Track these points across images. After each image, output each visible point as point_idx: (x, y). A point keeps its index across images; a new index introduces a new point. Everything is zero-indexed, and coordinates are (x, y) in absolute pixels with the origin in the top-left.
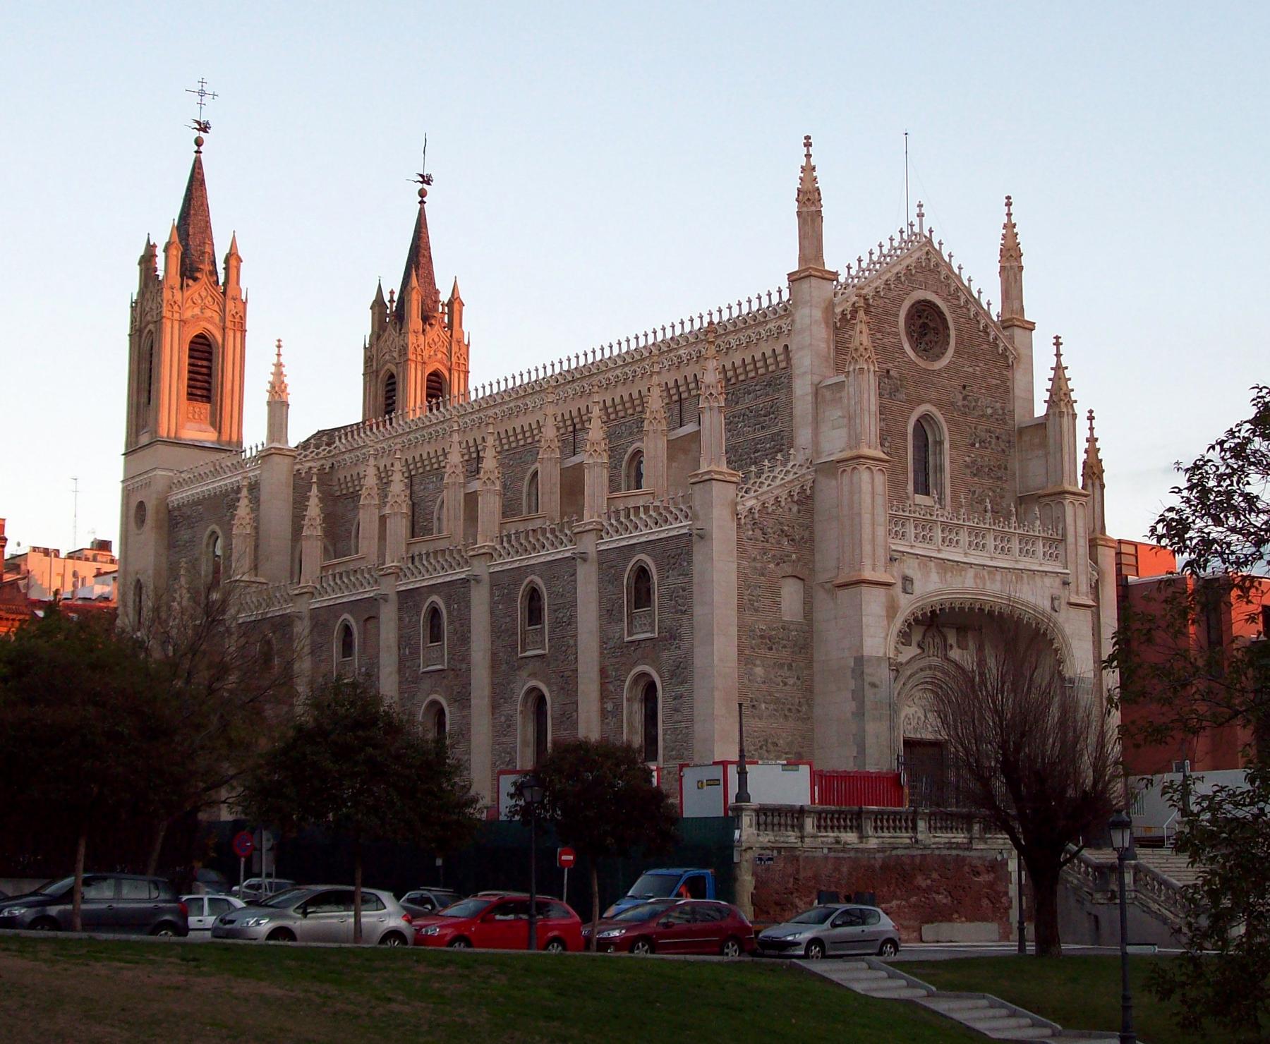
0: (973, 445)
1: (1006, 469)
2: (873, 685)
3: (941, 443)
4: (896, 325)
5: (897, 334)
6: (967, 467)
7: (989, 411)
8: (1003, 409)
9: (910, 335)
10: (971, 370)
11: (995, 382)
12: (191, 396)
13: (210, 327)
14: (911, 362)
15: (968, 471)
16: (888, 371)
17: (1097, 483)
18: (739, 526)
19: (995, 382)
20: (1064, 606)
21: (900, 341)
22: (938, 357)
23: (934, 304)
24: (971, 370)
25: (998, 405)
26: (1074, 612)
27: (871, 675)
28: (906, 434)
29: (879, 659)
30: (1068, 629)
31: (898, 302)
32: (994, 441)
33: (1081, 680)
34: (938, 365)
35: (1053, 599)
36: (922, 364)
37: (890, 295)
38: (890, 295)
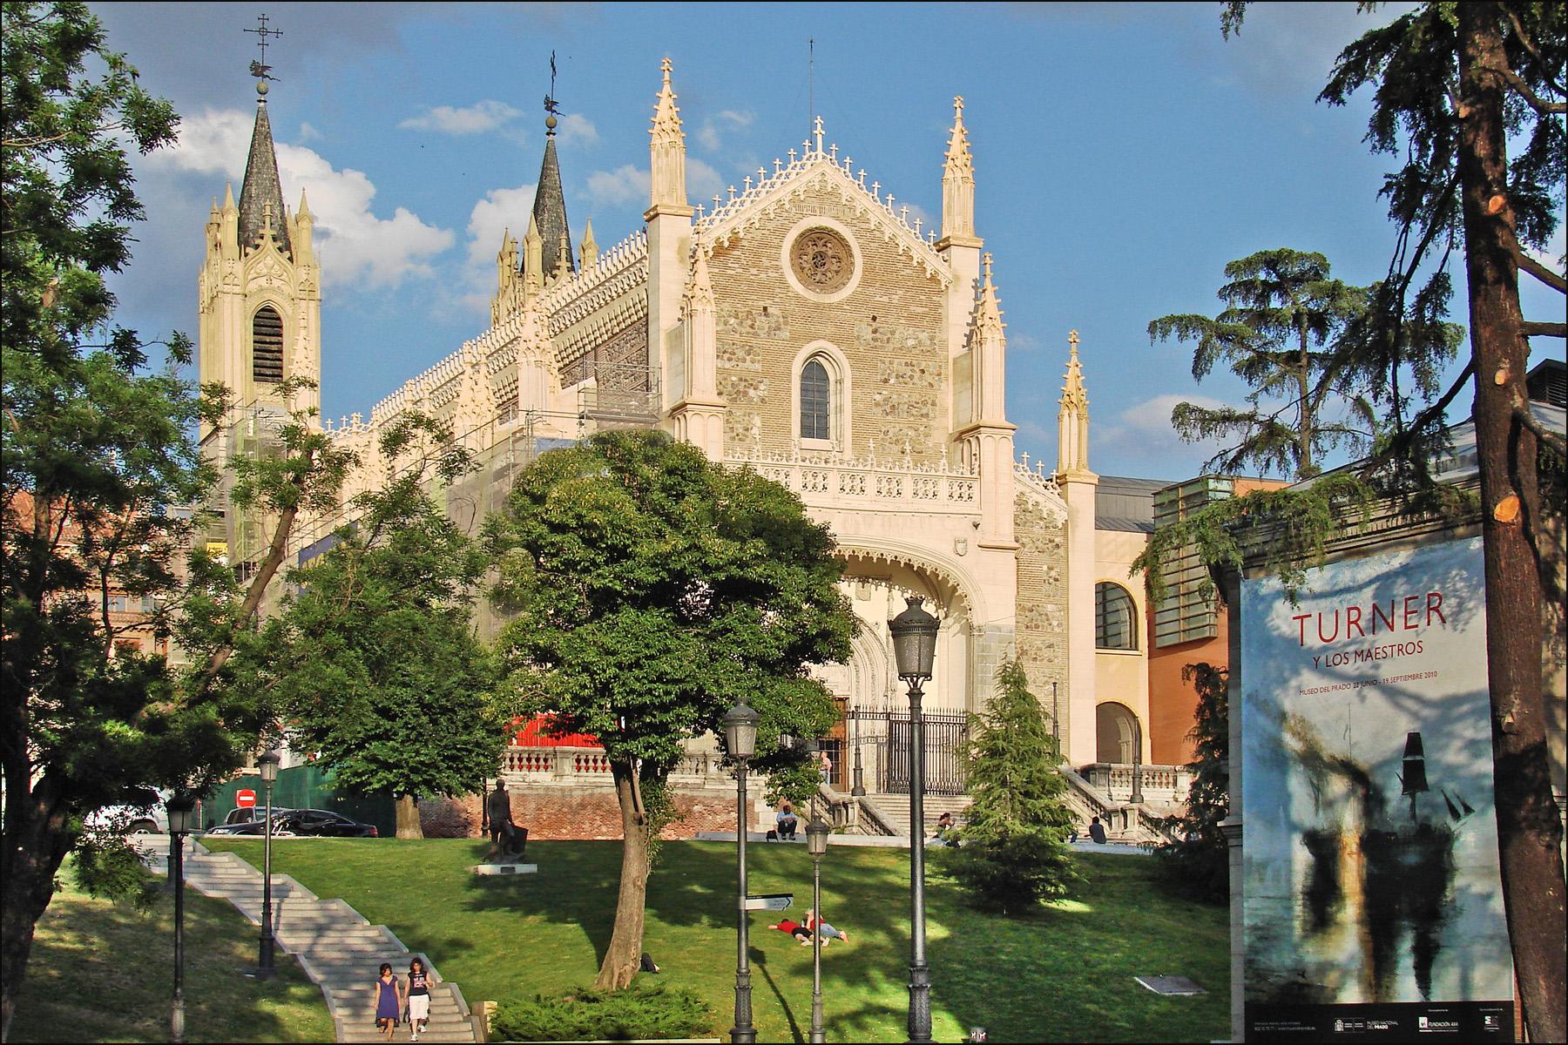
0: (886, 381)
1: (934, 404)
3: (840, 382)
5: (777, 268)
6: (877, 405)
7: (911, 342)
8: (932, 339)
9: (799, 269)
10: (885, 299)
11: (920, 310)
12: (259, 376)
13: (274, 297)
14: (797, 296)
15: (879, 410)
16: (765, 309)
17: (1074, 412)
19: (920, 310)
20: (972, 547)
22: (837, 288)
24: (885, 299)
25: (924, 336)
28: (789, 374)
31: (782, 232)
32: (917, 375)
34: (835, 298)
35: (957, 542)
36: (812, 296)
38: (771, 226)
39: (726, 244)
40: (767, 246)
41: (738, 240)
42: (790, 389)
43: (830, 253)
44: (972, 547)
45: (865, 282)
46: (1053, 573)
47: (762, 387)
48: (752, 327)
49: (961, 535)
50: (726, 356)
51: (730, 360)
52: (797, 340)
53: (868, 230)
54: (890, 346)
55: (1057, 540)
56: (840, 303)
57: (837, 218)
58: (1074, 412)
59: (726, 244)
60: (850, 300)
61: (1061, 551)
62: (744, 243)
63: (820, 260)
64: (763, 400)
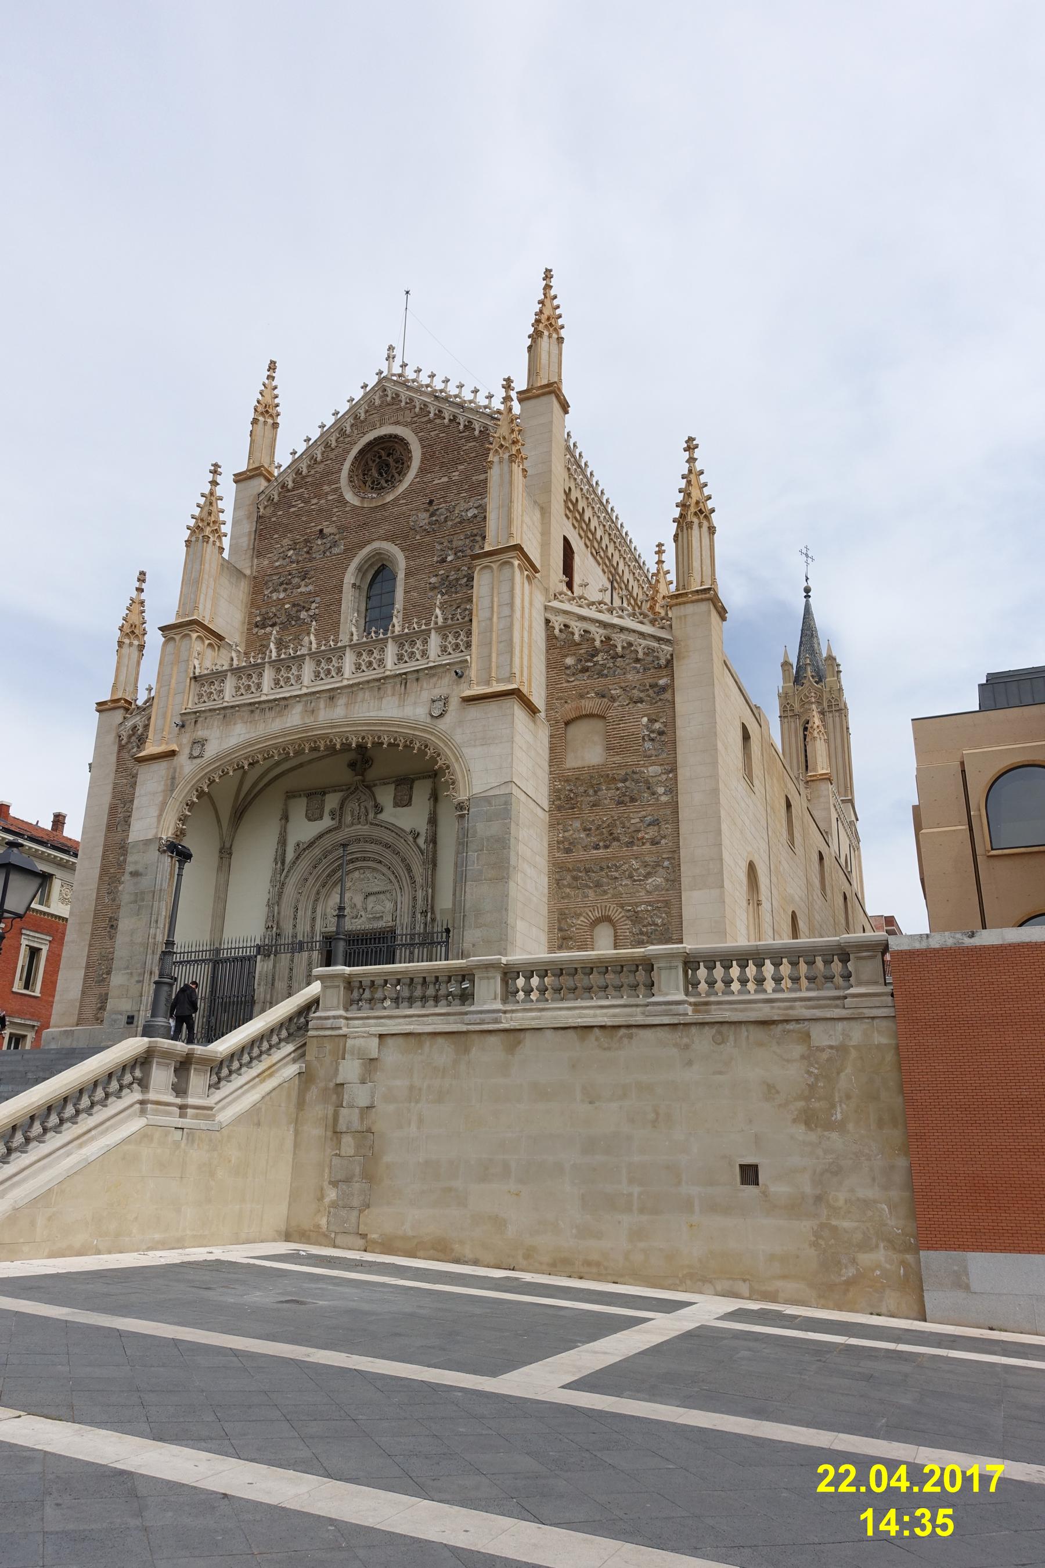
0: (444, 561)
2: (135, 874)
4: (338, 481)
6: (434, 588)
7: (470, 514)
10: (445, 479)
16: (321, 531)
18: (121, 748)
21: (341, 495)
23: (390, 436)
24: (445, 479)
26: (475, 712)
27: (136, 863)
29: (147, 842)
30: (458, 737)
33: (488, 800)
34: (389, 498)
37: (332, 455)
38: (332, 455)
39: (290, 485)
40: (330, 475)
41: (304, 477)
42: (339, 602)
43: (391, 460)
44: (454, 703)
45: (422, 470)
46: (657, 726)
47: (314, 605)
48: (308, 552)
49: (437, 692)
50: (281, 588)
51: (285, 590)
52: (350, 551)
53: (430, 421)
54: (450, 523)
55: (662, 682)
56: (397, 499)
57: (397, 423)
58: (705, 524)
59: (290, 485)
60: (404, 495)
61: (667, 696)
62: (309, 479)
63: (384, 467)
64: (313, 617)
